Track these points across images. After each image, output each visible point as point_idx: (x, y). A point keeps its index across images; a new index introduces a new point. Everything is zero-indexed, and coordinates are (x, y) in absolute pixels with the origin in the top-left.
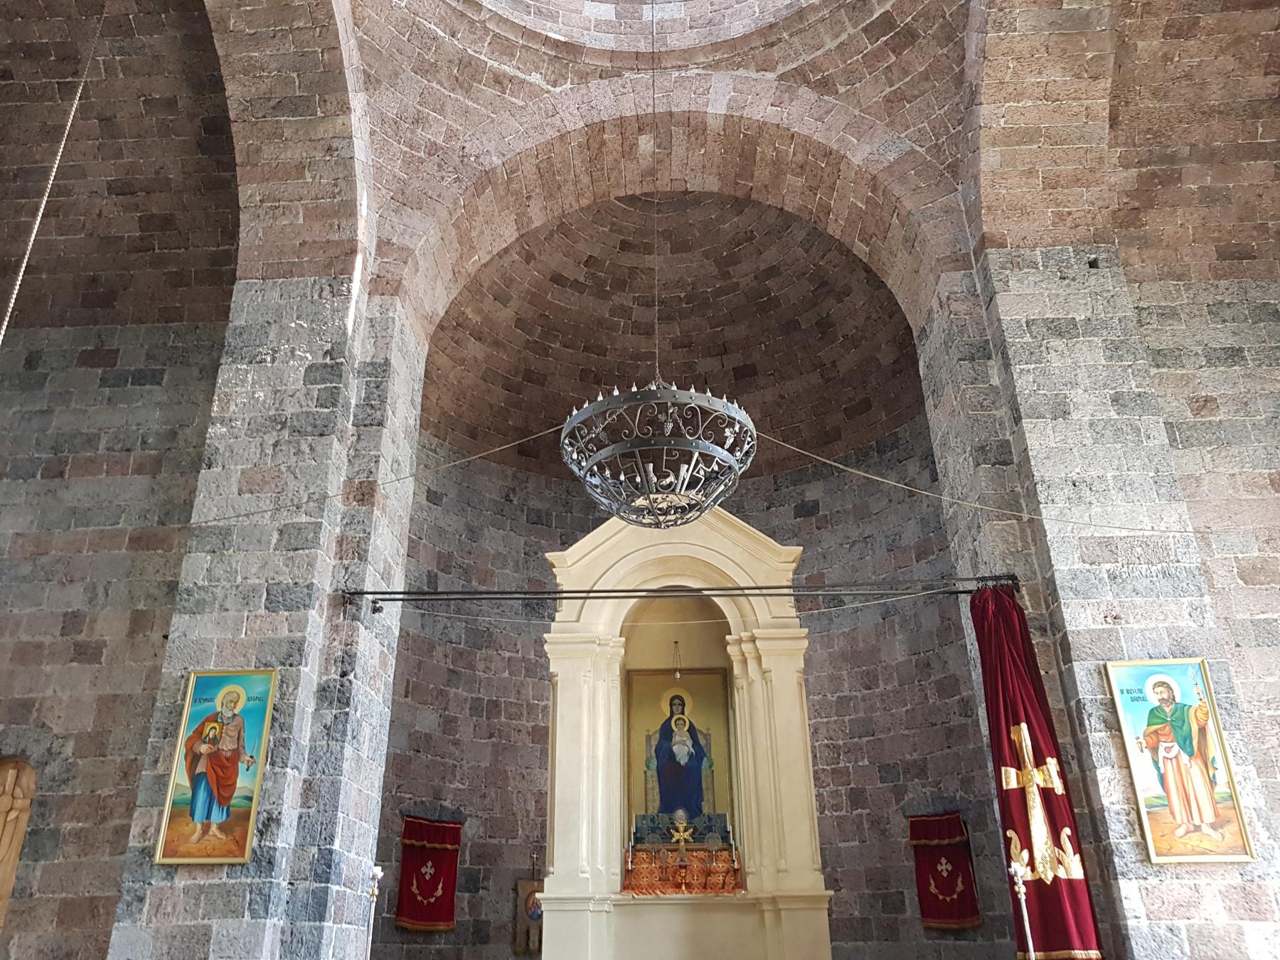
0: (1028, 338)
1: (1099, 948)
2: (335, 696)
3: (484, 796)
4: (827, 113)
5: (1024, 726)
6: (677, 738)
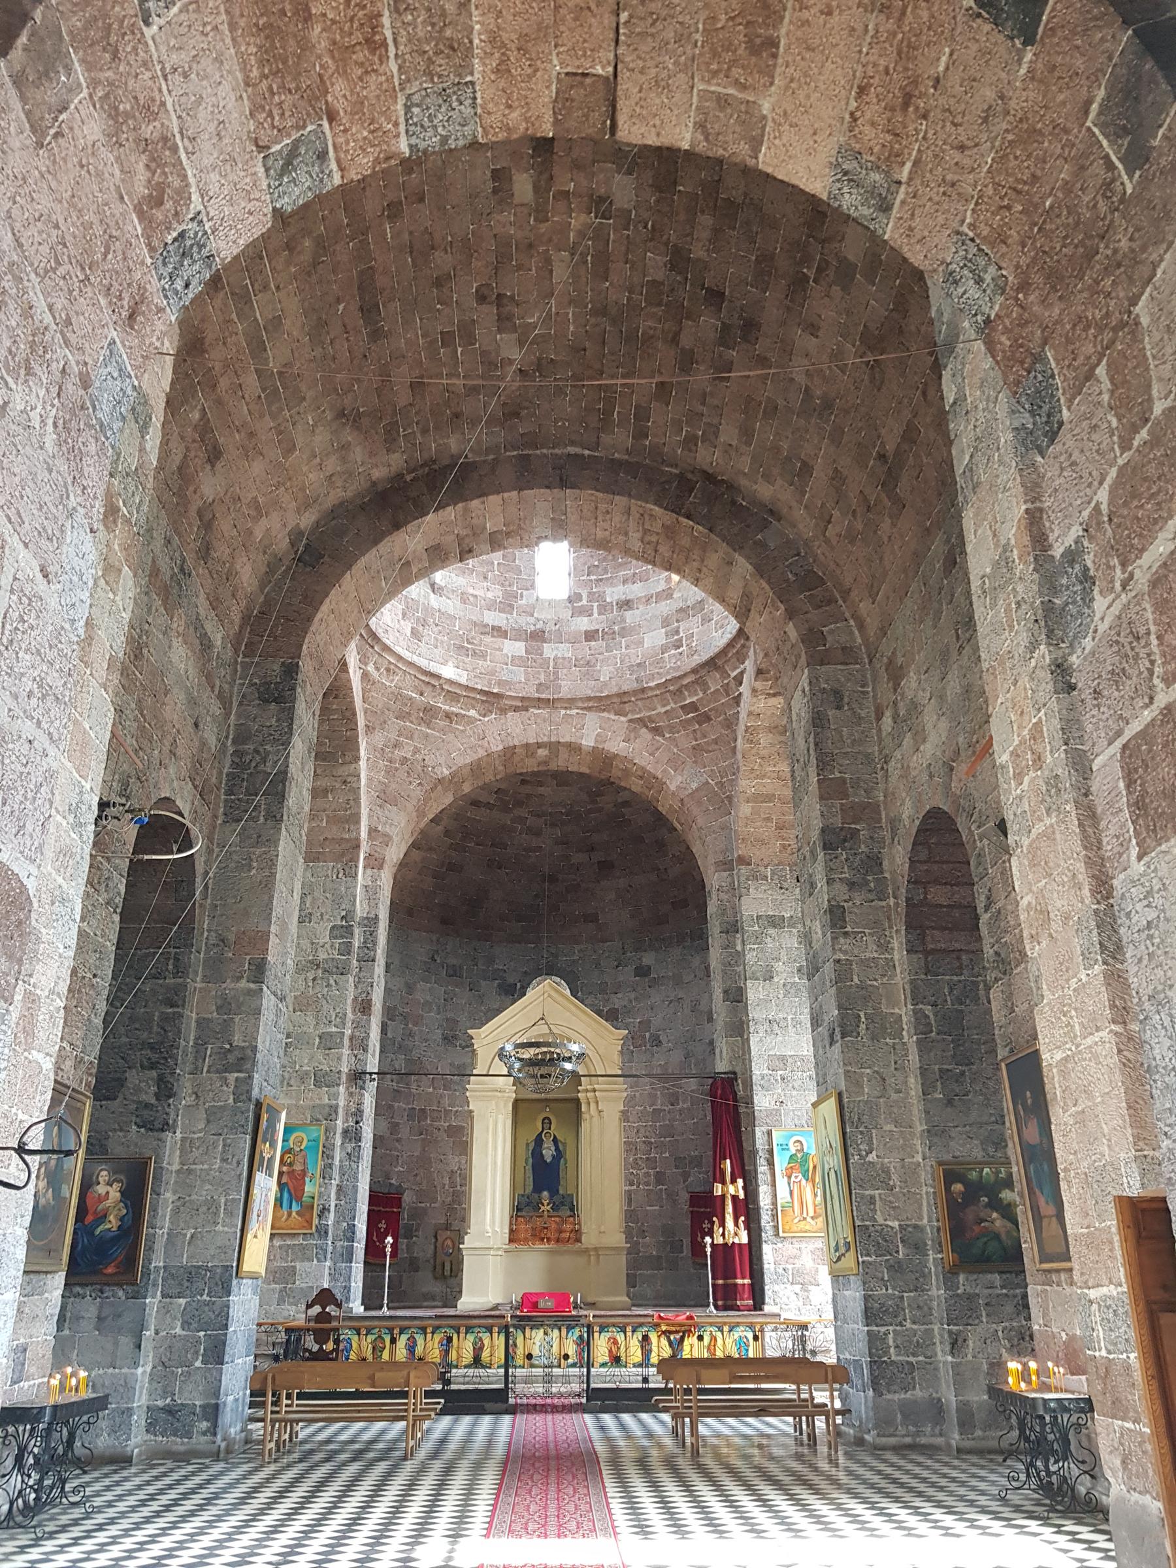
0: (756, 928)
2: (353, 1135)
3: (416, 1175)
4: (657, 749)
5: (728, 1161)
6: (545, 1145)
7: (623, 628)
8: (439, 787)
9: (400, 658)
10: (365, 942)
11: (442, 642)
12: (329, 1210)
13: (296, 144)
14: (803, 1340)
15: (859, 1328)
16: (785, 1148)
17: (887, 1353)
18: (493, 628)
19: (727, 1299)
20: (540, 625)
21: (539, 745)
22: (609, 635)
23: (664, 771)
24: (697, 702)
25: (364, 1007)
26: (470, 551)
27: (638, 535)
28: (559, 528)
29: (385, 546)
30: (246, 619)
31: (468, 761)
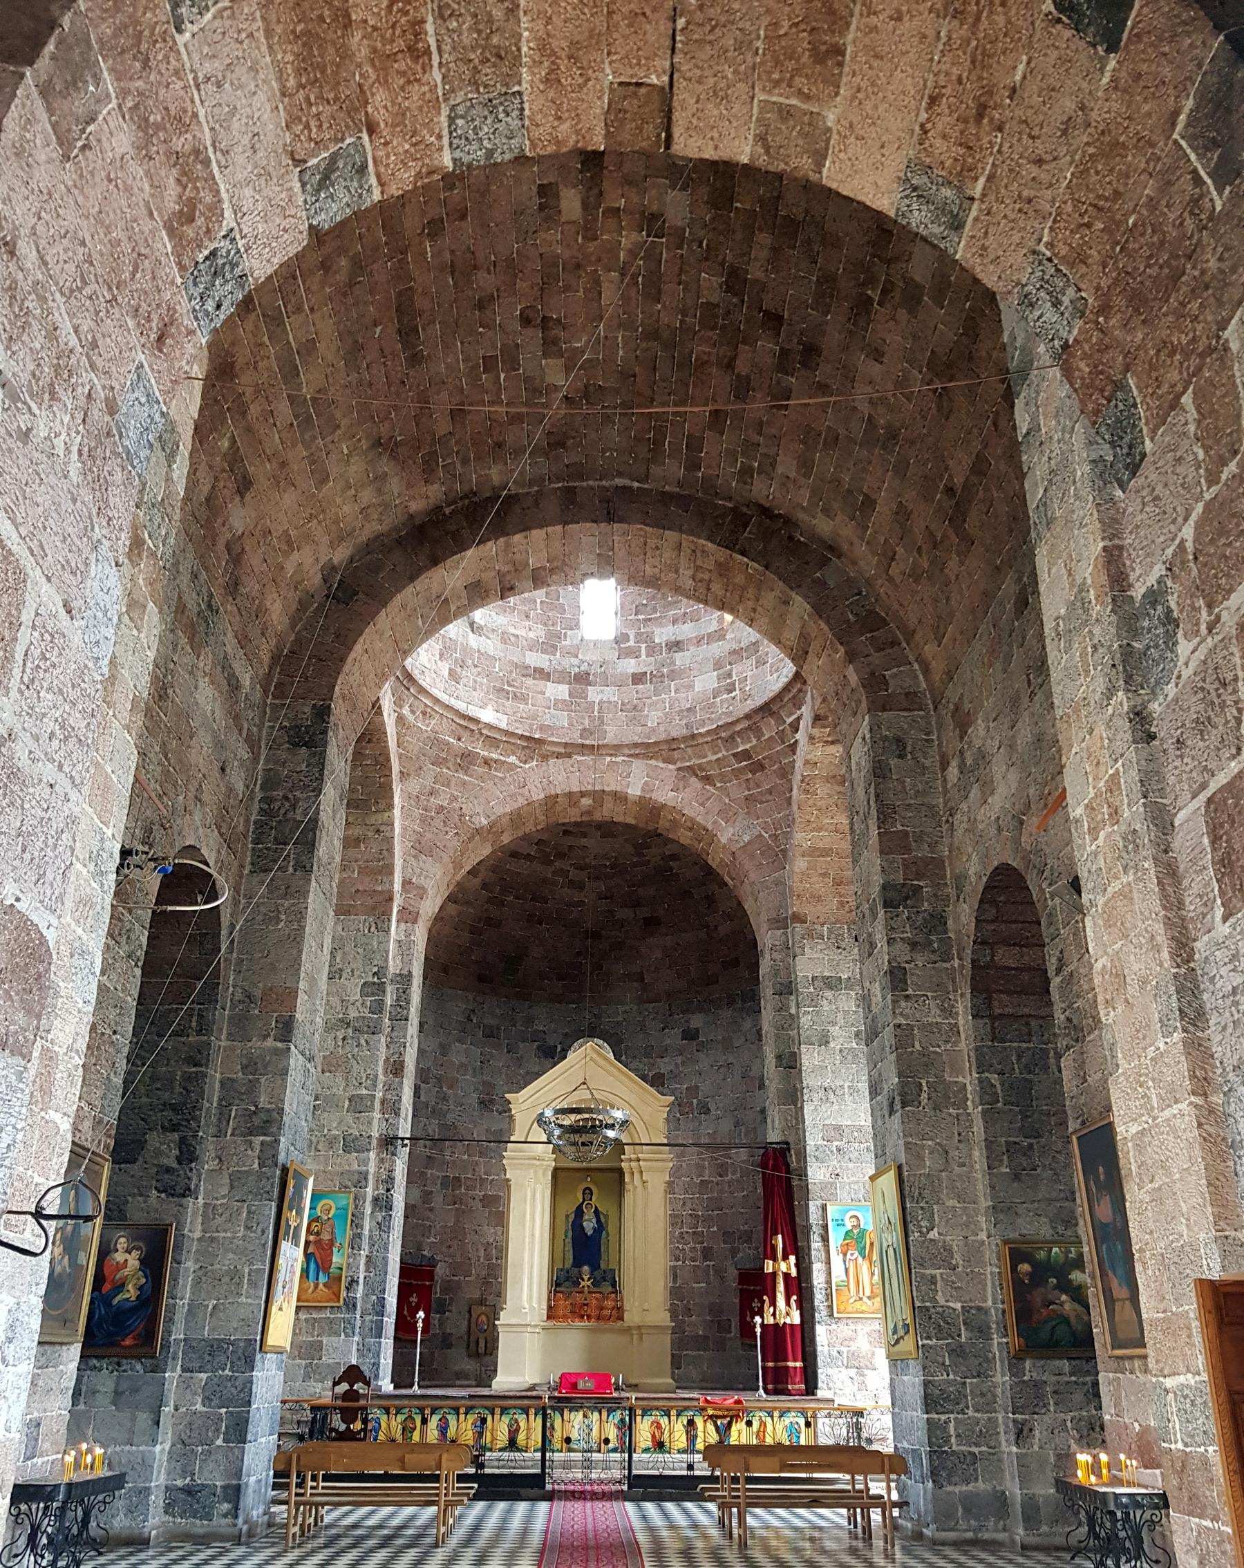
0: (812, 990)
1: (804, 1360)
2: (383, 1203)
5: (780, 1236)
7: (673, 671)
8: (477, 838)
9: (437, 701)
10: (397, 1000)
11: (481, 684)
12: (357, 1282)
13: (334, 158)
14: (858, 1427)
15: (918, 1415)
16: (840, 1223)
17: (947, 1442)
18: (535, 670)
19: (778, 1383)
20: (584, 667)
21: (583, 794)
22: (657, 678)
23: (715, 823)
24: (750, 749)
25: (397, 1069)
26: (512, 588)
27: (690, 572)
28: (605, 565)
29: (421, 583)
30: (275, 658)
31: (508, 809)
